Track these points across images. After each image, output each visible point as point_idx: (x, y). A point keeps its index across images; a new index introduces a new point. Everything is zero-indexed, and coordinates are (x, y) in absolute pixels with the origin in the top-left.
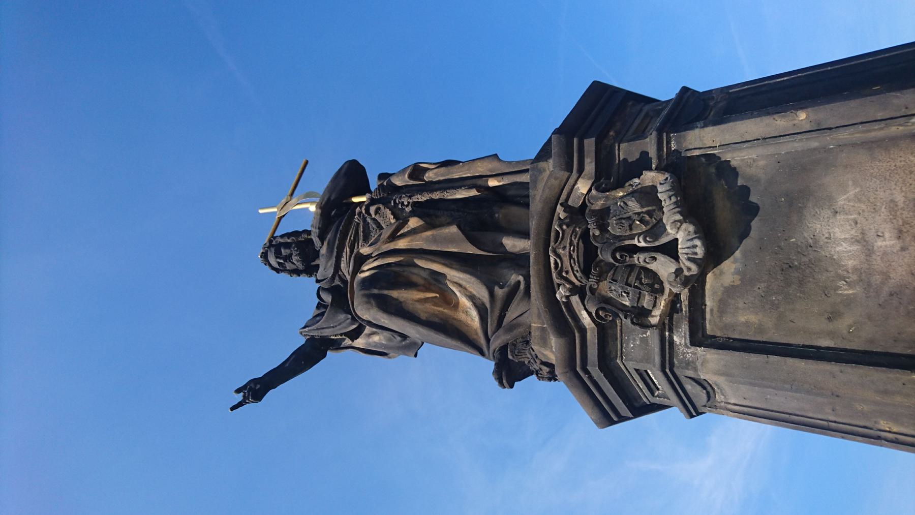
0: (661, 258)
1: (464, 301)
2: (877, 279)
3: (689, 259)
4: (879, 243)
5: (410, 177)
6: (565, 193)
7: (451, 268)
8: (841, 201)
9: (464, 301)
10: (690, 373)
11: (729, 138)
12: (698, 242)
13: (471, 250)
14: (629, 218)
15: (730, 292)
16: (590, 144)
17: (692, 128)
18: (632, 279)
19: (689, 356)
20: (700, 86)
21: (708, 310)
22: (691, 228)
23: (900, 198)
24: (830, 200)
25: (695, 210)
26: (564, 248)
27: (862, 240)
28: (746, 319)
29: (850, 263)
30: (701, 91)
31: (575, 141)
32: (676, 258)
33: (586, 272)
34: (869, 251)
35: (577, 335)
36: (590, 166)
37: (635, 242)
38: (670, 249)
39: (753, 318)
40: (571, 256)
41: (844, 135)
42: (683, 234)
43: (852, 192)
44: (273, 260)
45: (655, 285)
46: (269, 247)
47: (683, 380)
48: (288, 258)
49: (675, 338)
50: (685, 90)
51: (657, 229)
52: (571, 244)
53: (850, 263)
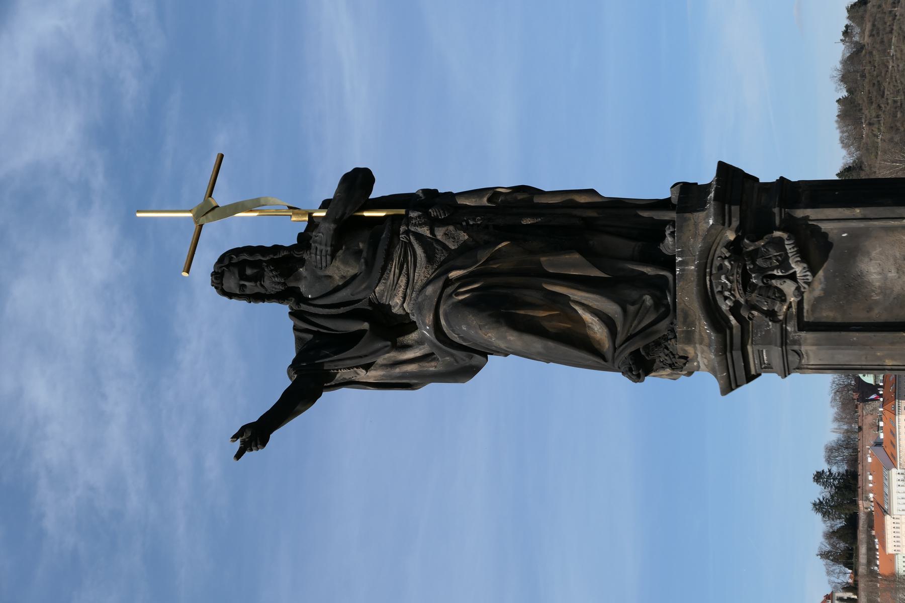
0: (789, 282)
1: (587, 317)
2: (888, 292)
3: (805, 283)
4: (890, 275)
5: (489, 200)
6: (719, 238)
7: (579, 290)
8: (874, 254)
9: (587, 317)
10: (796, 348)
11: (820, 217)
12: (808, 273)
13: (596, 273)
14: (770, 258)
15: (818, 300)
16: (735, 209)
17: (799, 208)
18: (770, 294)
19: (796, 338)
20: (794, 178)
21: (805, 311)
22: (805, 265)
23: (898, 255)
24: (868, 253)
25: (804, 257)
26: (733, 275)
28: (827, 314)
30: (793, 180)
31: (727, 207)
32: (797, 282)
33: (745, 290)
34: (886, 278)
35: (728, 332)
36: (735, 223)
37: (775, 272)
38: (793, 277)
39: (831, 314)
40: (737, 281)
41: (876, 223)
42: (798, 269)
43: (878, 250)
44: (231, 283)
45: (782, 297)
46: (227, 266)
47: (790, 352)
48: (257, 278)
49: (789, 328)
50: (782, 178)
51: (784, 264)
52: (737, 273)
53: (877, 284)
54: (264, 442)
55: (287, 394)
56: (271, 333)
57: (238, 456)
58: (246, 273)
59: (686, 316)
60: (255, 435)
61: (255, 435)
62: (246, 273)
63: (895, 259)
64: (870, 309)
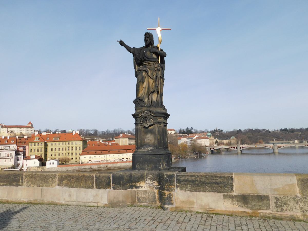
8: (151, 136)
24: (151, 135)
27: (148, 137)
29: (147, 137)
34: (148, 138)
54: (121, 45)
55: (130, 47)
56: (140, 43)
57: (118, 41)
58: (149, 37)
59: (142, 108)
60: (122, 43)
61: (122, 43)
62: (149, 37)
63: (150, 139)
64: (143, 136)
